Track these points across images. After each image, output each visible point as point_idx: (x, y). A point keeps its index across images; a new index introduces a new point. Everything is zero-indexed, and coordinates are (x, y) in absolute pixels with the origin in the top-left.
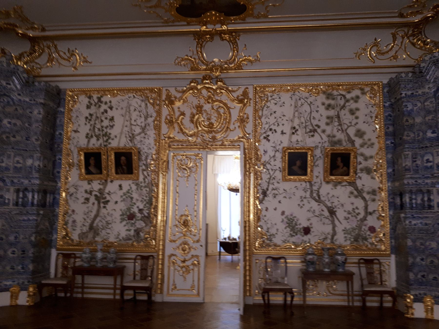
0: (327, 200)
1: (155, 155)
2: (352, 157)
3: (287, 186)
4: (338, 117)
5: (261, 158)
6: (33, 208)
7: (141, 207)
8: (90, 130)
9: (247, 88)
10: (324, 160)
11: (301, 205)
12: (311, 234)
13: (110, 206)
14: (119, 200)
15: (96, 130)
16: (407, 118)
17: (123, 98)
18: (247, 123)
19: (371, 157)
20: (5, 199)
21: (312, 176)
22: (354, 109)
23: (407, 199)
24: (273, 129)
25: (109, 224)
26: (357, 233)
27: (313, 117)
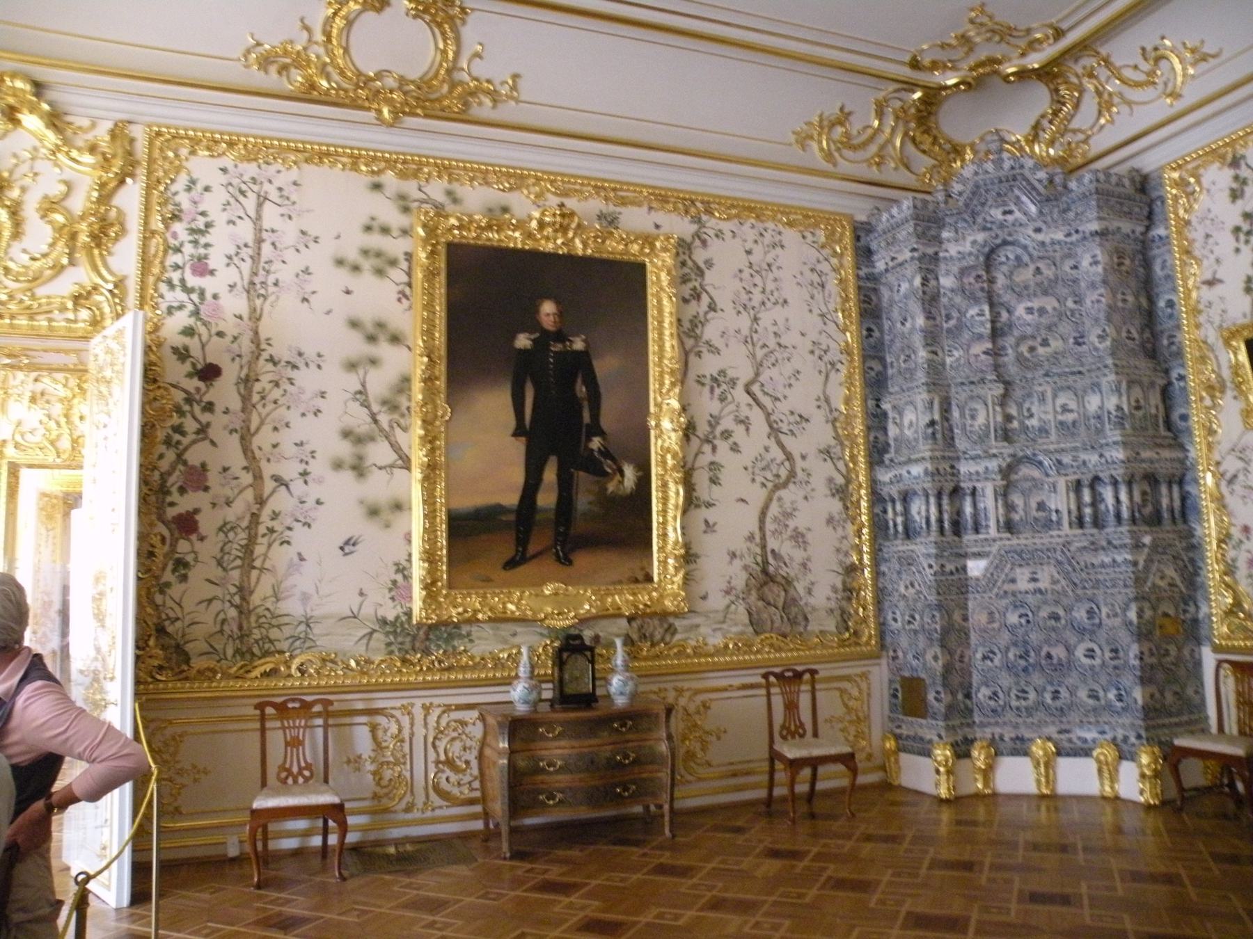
20: (1050, 510)
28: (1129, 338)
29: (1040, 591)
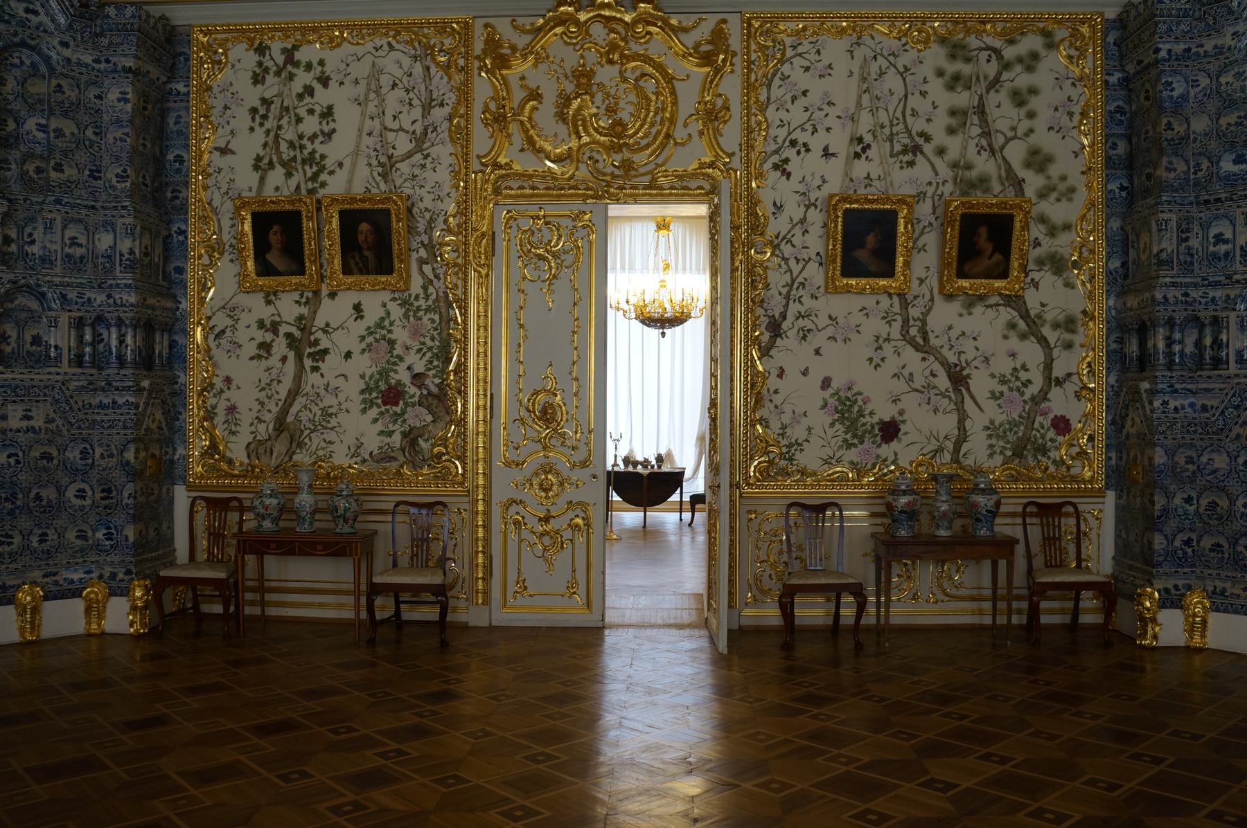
1: (454, 216)
2: (1017, 225)
4: (981, 110)
5: (765, 226)
6: (123, 372)
7: (419, 368)
8: (265, 145)
9: (724, 21)
10: (944, 234)
12: (900, 441)
13: (331, 364)
14: (356, 347)
15: (284, 146)
16: (1172, 120)
17: (359, 50)
18: (725, 122)
19: (1067, 227)
21: (907, 281)
22: (1024, 92)
23: (1159, 341)
24: (801, 141)
25: (330, 415)
26: (1020, 434)
27: (913, 110)
28: (144, 184)
29: (33, 428)
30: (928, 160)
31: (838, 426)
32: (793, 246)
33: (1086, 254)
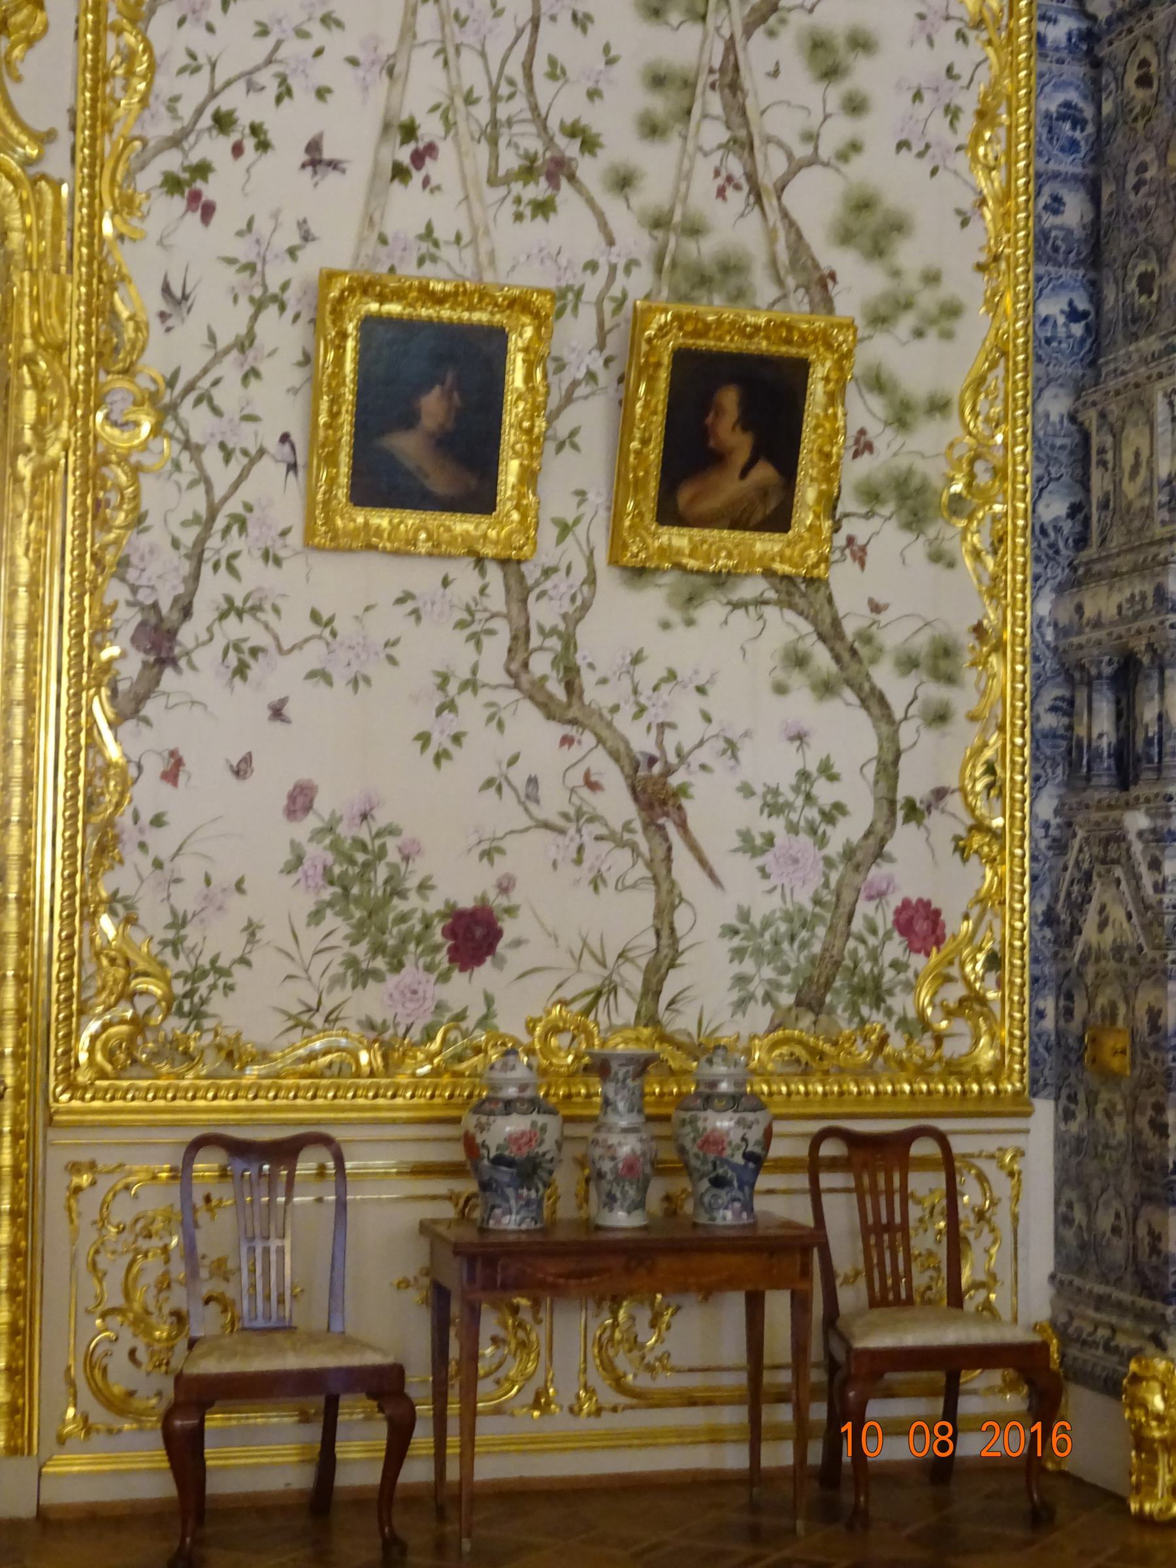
0: (628, 709)
2: (817, 390)
3: (338, 583)
4: (730, 81)
10: (625, 404)
11: (440, 740)
12: (500, 964)
18: (30, 42)
19: (938, 406)
22: (840, 42)
26: (817, 948)
27: (552, 62)
30: (590, 202)
31: (331, 920)
32: (216, 411)
33: (983, 479)
